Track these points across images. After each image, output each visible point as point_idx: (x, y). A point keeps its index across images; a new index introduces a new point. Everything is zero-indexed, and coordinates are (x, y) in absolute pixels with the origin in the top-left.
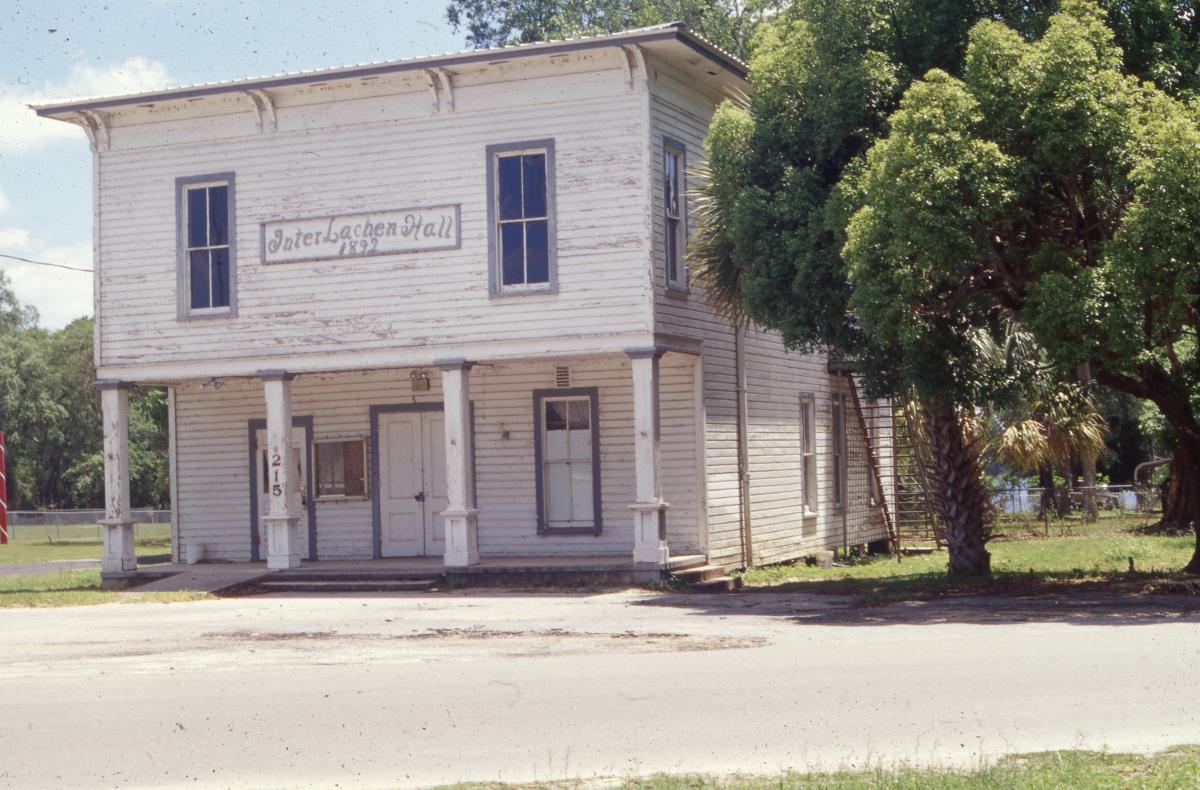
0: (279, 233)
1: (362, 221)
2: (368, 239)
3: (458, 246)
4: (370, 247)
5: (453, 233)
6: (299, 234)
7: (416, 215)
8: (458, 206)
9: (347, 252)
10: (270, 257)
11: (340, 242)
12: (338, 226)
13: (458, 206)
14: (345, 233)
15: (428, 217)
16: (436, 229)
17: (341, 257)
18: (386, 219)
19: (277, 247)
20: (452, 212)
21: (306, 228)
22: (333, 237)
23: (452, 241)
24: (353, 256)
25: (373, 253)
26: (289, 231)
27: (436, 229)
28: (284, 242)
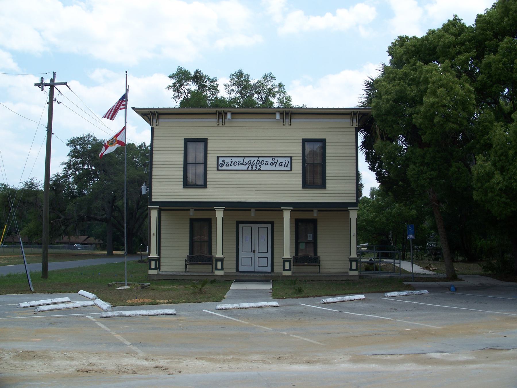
0: (224, 161)
1: (256, 159)
2: (258, 165)
3: (291, 170)
4: (258, 168)
5: (289, 165)
6: (232, 161)
7: (276, 159)
8: (291, 157)
9: (250, 168)
10: (220, 168)
11: (247, 165)
12: (246, 160)
13: (291, 157)
14: (249, 163)
15: (280, 160)
16: (283, 164)
17: (247, 170)
18: (265, 159)
19: (223, 166)
20: (289, 159)
21: (235, 160)
22: (244, 163)
23: (289, 168)
24: (252, 170)
25: (260, 170)
26: (228, 160)
27: (283, 164)
28: (226, 163)
